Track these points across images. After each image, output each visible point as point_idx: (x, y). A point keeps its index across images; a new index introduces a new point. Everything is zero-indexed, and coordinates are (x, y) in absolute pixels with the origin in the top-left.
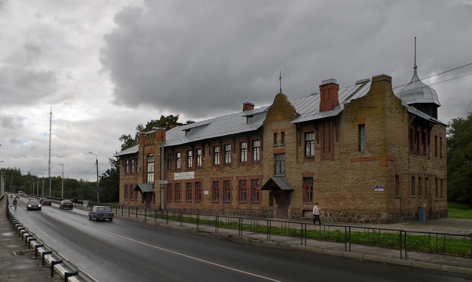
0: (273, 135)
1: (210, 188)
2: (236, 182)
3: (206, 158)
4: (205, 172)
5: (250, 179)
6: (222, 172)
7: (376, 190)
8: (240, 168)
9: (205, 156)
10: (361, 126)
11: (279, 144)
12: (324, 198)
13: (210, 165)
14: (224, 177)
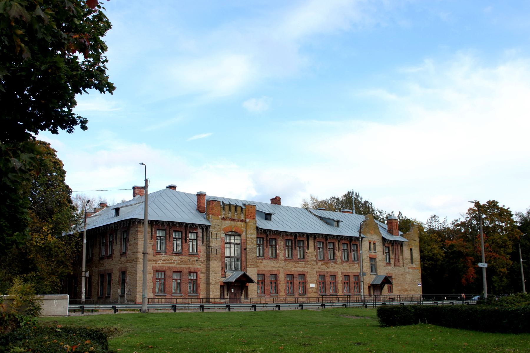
0: (368, 243)
1: (315, 281)
2: (341, 276)
3: (310, 250)
4: (309, 265)
5: (353, 275)
6: (328, 267)
7: (419, 286)
8: (344, 264)
9: (309, 248)
10: (411, 250)
11: (372, 250)
12: (398, 290)
13: (314, 258)
14: (330, 272)
